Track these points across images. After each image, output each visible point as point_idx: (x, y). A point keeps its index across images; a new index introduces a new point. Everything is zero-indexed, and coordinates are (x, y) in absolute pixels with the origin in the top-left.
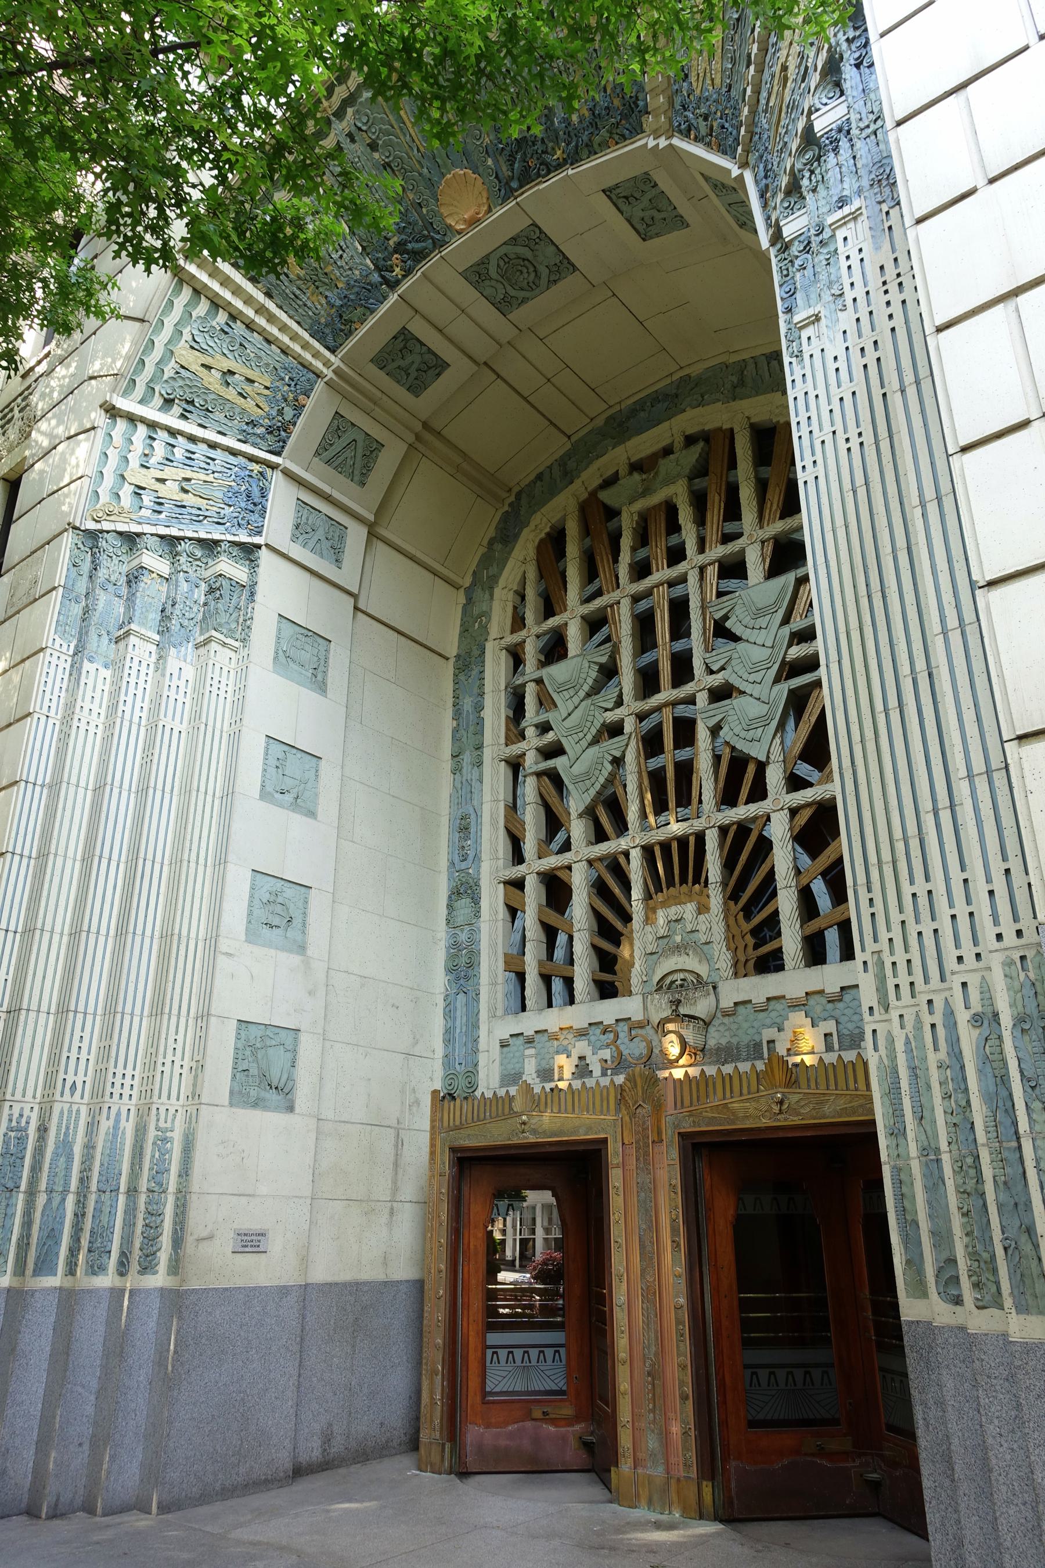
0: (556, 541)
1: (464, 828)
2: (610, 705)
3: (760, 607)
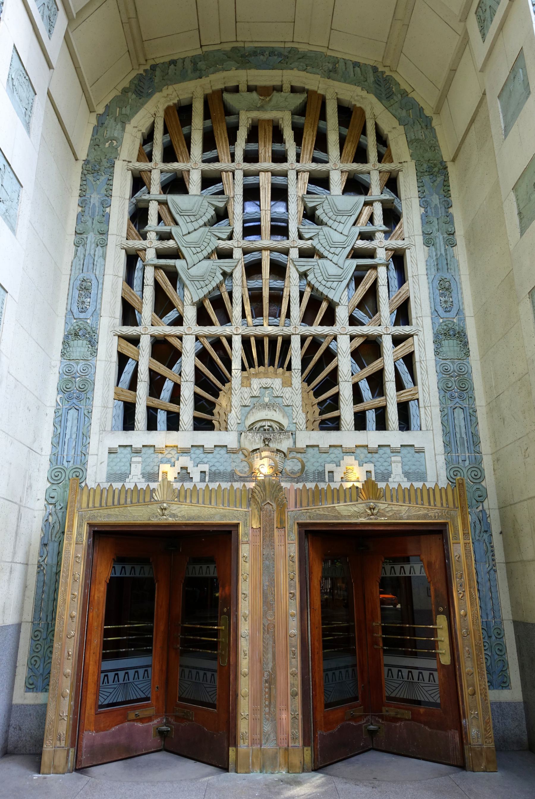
0: (182, 112)
1: (84, 289)
2: (225, 237)
3: (340, 209)
